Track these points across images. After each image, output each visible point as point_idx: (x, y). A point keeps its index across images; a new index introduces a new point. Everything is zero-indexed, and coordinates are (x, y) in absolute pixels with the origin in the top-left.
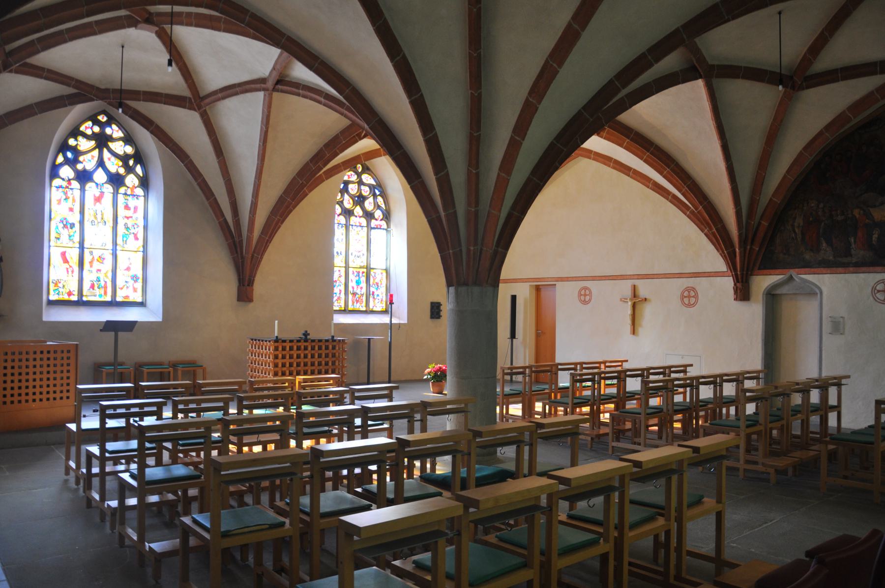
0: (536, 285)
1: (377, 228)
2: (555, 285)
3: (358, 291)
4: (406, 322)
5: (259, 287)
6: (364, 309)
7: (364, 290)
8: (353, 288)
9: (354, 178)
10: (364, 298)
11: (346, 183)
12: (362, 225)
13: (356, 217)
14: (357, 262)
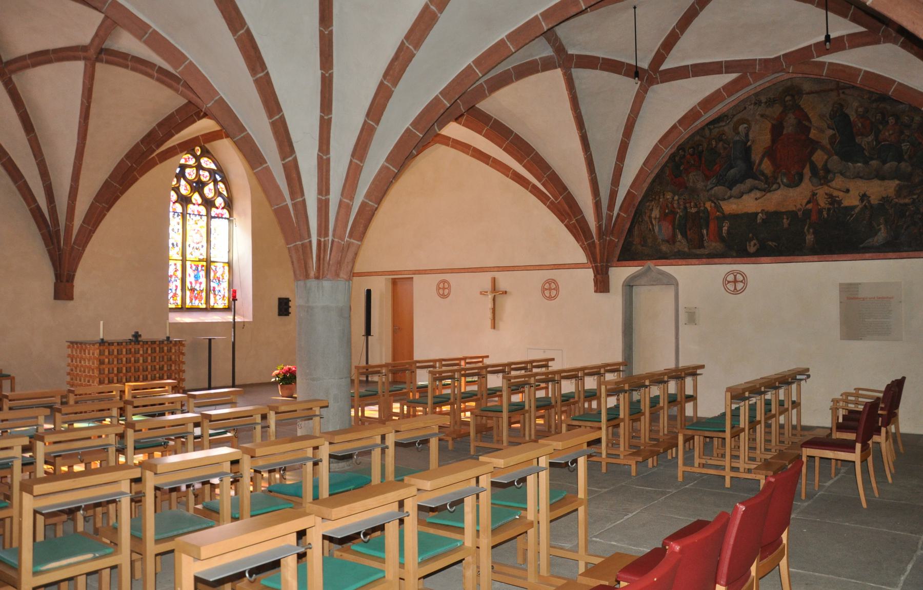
0: (392, 279)
1: (218, 217)
2: (412, 278)
3: (197, 287)
4: (251, 320)
5: (81, 283)
6: (204, 306)
7: (204, 286)
8: (191, 283)
9: (192, 162)
10: (204, 294)
11: (183, 167)
13: (194, 204)
14: (195, 254)
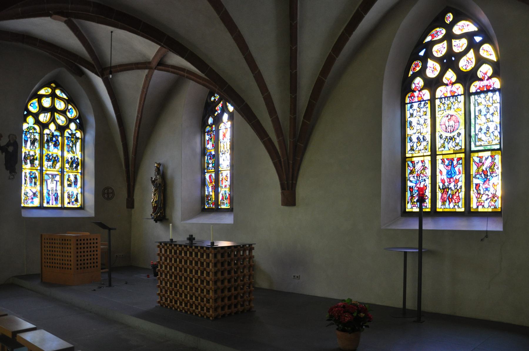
3: (452, 186)
8: (443, 181)
12: (456, 94)
13: (447, 85)
